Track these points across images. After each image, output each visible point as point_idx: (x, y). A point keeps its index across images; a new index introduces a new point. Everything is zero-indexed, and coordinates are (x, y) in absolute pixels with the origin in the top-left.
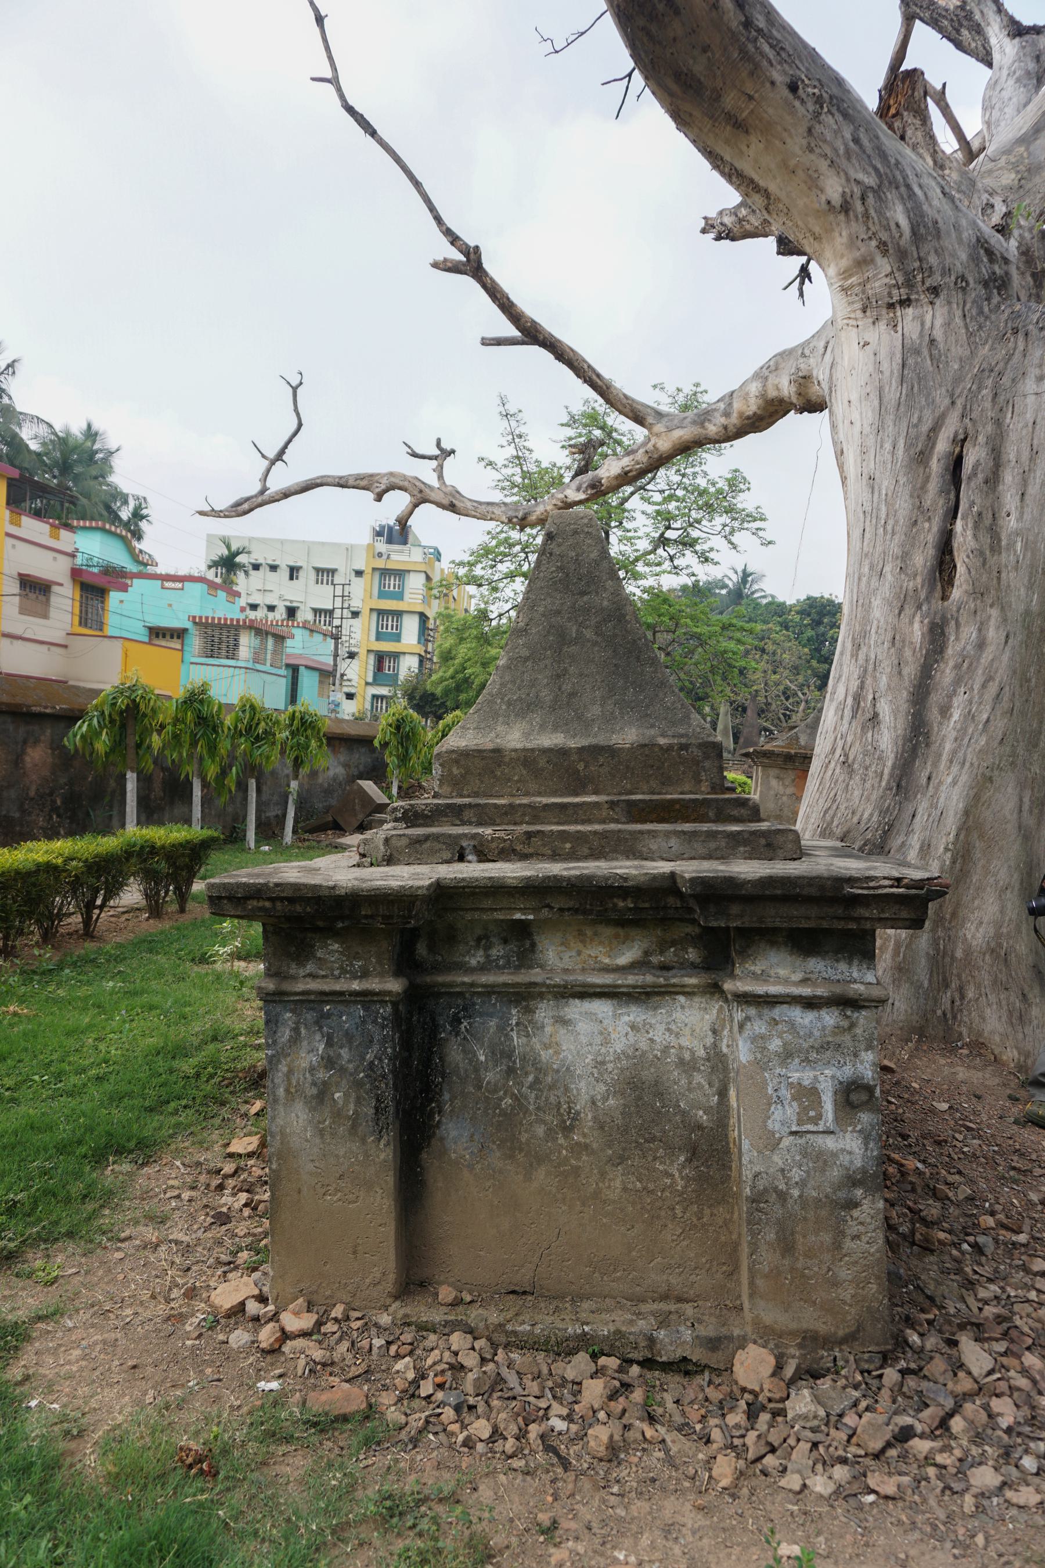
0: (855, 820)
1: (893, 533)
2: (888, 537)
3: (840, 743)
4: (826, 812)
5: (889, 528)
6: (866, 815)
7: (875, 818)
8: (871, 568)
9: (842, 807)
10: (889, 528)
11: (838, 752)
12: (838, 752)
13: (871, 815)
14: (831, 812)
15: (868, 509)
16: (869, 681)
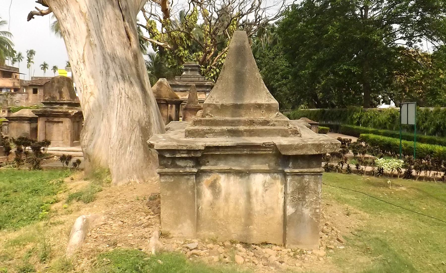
0: (139, 115)
1: (111, 21)
2: (109, 21)
3: (123, 92)
4: (129, 114)
5: (108, 18)
6: (142, 114)
7: (145, 114)
8: (106, 31)
9: (134, 112)
10: (108, 18)
11: (124, 94)
12: (124, 94)
13: (143, 114)
14: (131, 114)
15: (97, 8)
16: (124, 71)
